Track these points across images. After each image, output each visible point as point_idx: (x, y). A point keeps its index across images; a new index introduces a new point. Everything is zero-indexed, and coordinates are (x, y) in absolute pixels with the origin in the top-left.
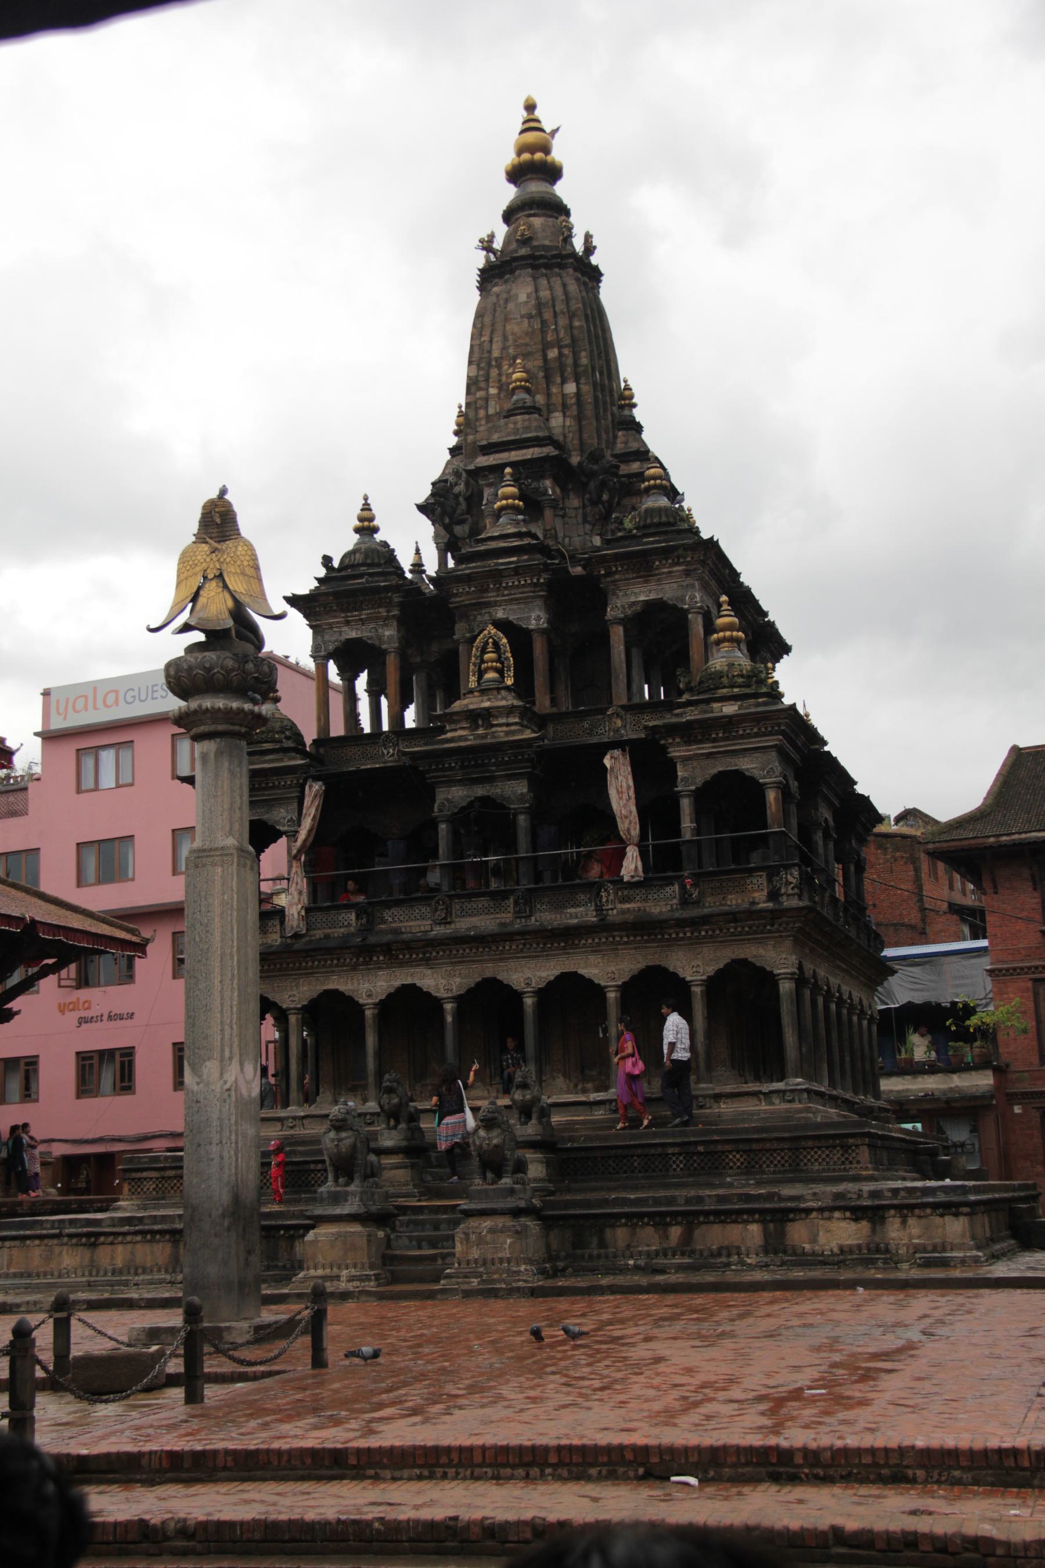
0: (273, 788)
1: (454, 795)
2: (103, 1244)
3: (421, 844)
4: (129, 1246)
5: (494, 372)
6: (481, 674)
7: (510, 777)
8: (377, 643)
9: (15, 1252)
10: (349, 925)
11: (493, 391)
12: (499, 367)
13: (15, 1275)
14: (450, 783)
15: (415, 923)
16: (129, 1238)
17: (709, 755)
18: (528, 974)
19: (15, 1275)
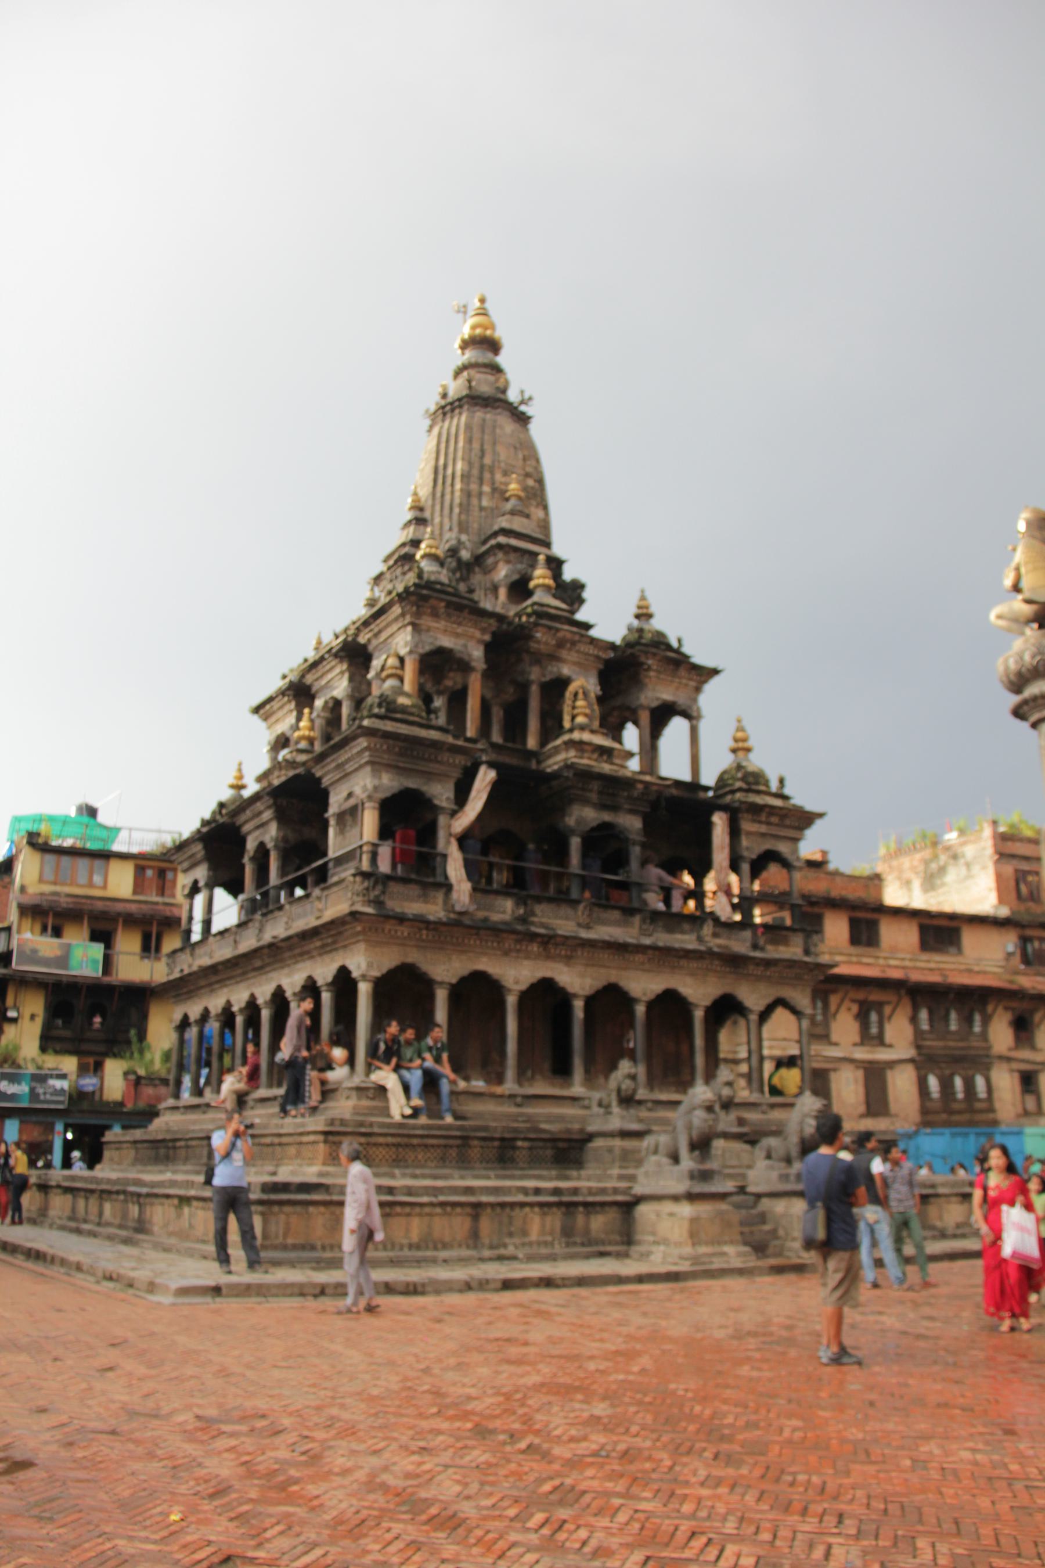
0: (438, 762)
1: (584, 815)
2: (399, 1215)
3: (559, 852)
4: (426, 1219)
5: (487, 476)
6: (573, 718)
7: (631, 812)
8: (466, 658)
9: (294, 1219)
10: (504, 912)
11: (486, 489)
12: (492, 473)
13: (295, 1247)
14: (586, 802)
15: (564, 923)
16: (427, 1210)
17: (763, 835)
18: (643, 985)
19: (295, 1247)
